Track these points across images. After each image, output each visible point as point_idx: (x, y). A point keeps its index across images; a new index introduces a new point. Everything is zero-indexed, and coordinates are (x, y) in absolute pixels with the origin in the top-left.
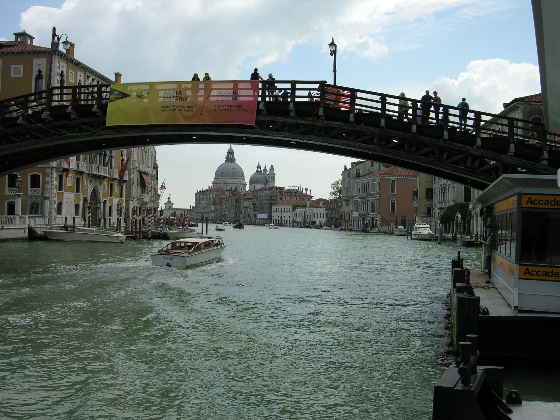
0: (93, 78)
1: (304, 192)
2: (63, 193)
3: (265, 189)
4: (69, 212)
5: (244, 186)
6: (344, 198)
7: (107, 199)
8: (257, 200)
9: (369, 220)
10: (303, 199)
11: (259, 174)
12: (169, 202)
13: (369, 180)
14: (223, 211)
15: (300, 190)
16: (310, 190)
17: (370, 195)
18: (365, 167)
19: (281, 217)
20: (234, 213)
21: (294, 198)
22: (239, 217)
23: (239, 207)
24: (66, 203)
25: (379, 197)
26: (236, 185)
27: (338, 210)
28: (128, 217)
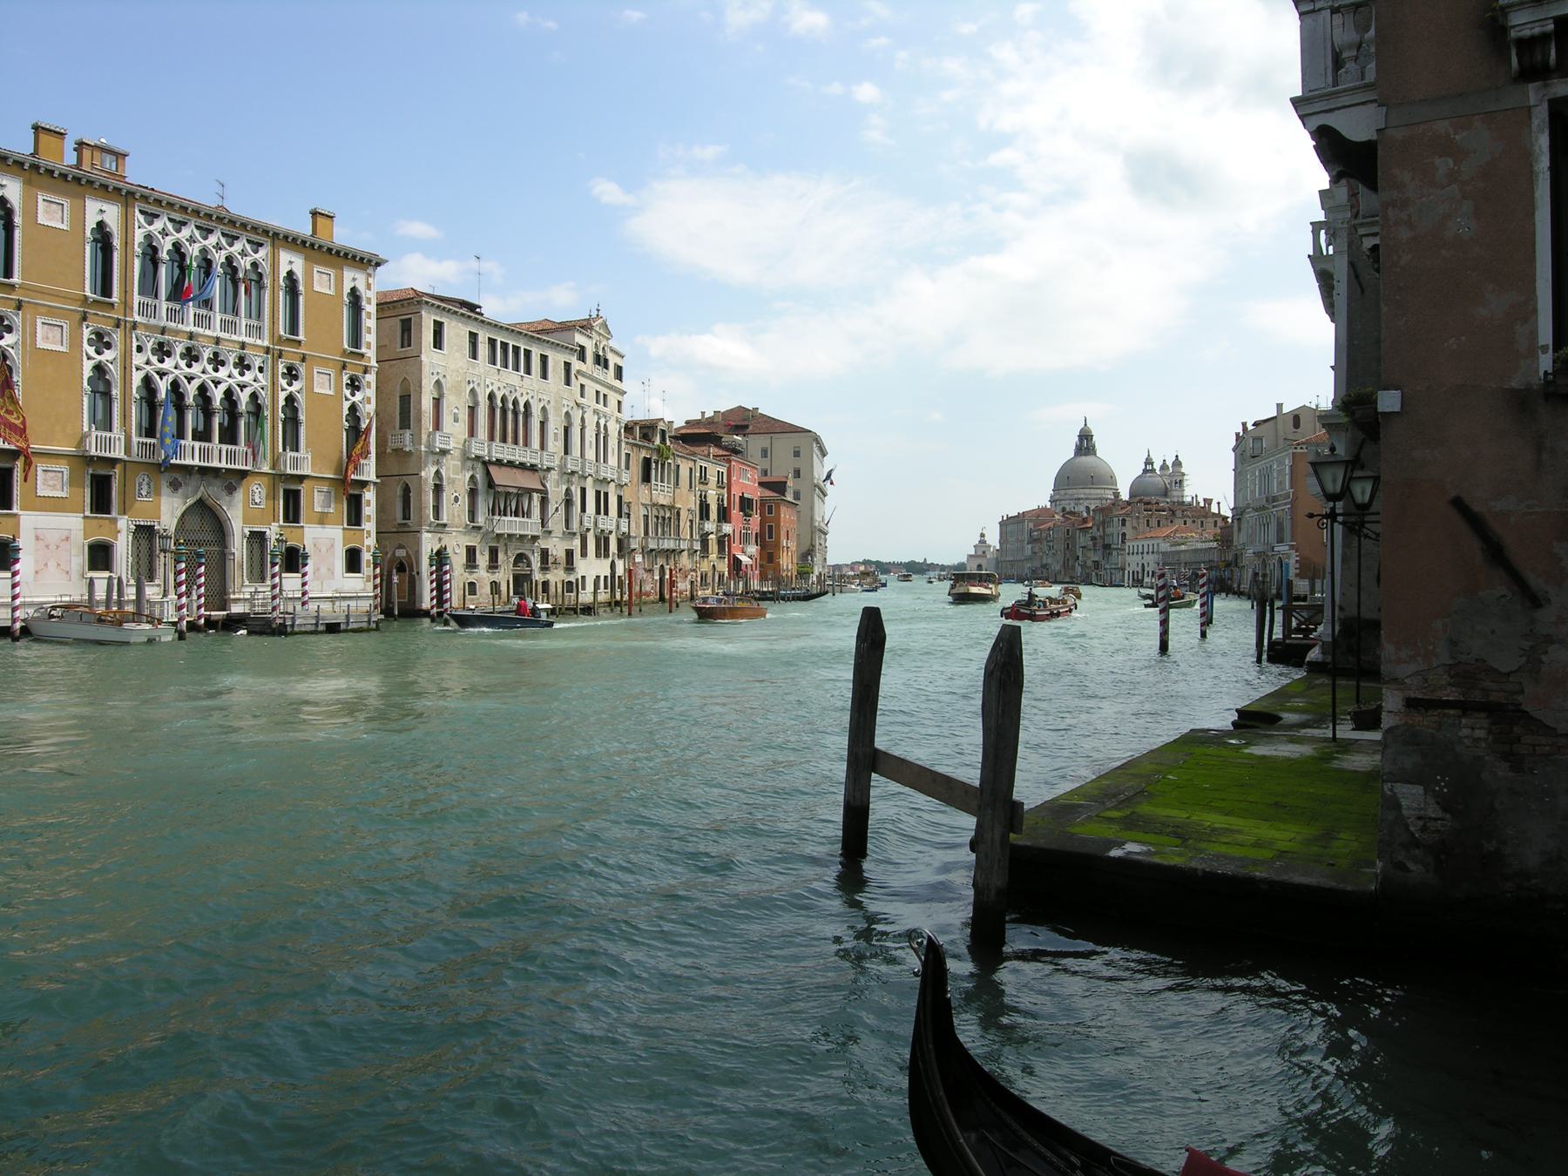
0: (178, 219)
2: (15, 515)
3: (1113, 504)
4: (52, 565)
7: (273, 531)
12: (982, 542)
15: (1198, 503)
16: (1219, 503)
17: (1275, 499)
18: (1276, 430)
21: (1179, 523)
22: (1073, 567)
24: (37, 538)
25: (1291, 502)
26: (1098, 501)
28: (418, 573)
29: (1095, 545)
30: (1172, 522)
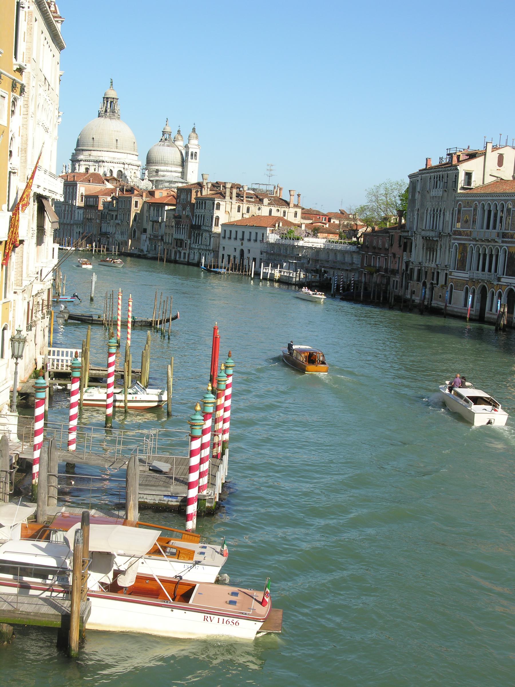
1: (285, 196)
5: (136, 168)
6: (423, 233)
8: (184, 210)
9: (500, 292)
10: (284, 212)
11: (168, 146)
13: (508, 200)
14: (104, 225)
16: (299, 195)
17: (504, 235)
19: (242, 251)
20: (129, 231)
22: (139, 239)
23: (139, 219)
27: (394, 255)
29: (178, 224)
30: (259, 209)
